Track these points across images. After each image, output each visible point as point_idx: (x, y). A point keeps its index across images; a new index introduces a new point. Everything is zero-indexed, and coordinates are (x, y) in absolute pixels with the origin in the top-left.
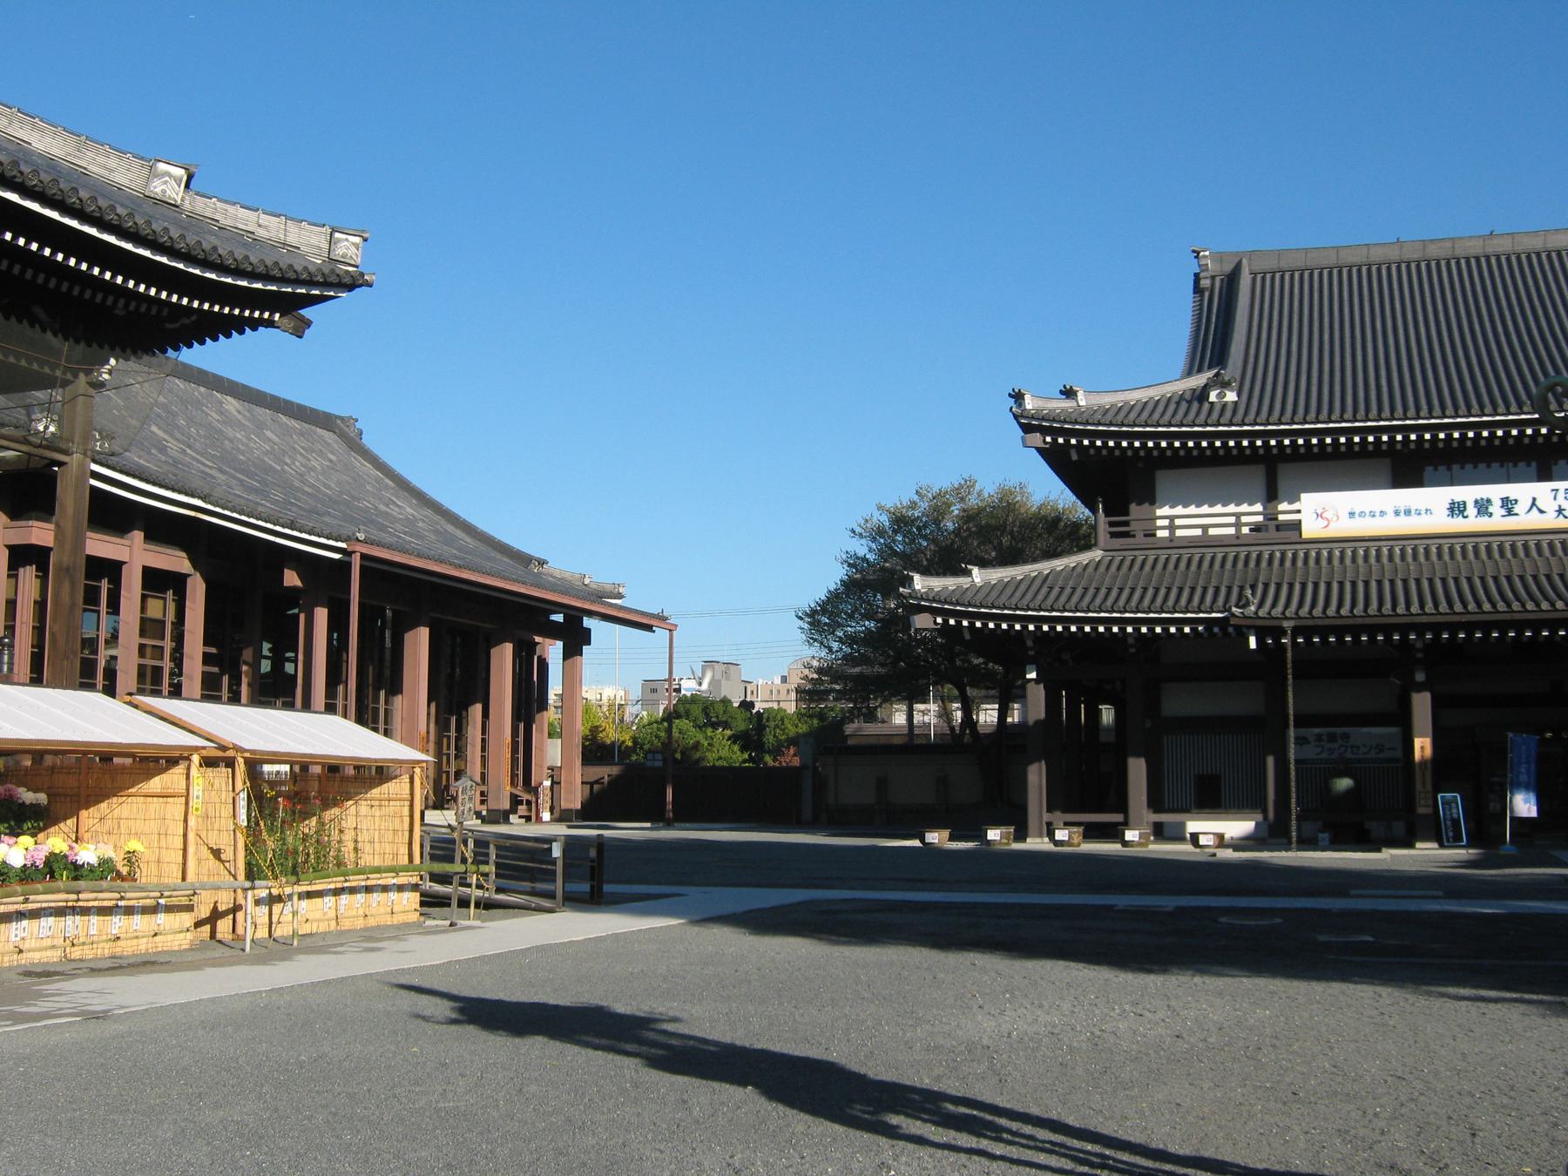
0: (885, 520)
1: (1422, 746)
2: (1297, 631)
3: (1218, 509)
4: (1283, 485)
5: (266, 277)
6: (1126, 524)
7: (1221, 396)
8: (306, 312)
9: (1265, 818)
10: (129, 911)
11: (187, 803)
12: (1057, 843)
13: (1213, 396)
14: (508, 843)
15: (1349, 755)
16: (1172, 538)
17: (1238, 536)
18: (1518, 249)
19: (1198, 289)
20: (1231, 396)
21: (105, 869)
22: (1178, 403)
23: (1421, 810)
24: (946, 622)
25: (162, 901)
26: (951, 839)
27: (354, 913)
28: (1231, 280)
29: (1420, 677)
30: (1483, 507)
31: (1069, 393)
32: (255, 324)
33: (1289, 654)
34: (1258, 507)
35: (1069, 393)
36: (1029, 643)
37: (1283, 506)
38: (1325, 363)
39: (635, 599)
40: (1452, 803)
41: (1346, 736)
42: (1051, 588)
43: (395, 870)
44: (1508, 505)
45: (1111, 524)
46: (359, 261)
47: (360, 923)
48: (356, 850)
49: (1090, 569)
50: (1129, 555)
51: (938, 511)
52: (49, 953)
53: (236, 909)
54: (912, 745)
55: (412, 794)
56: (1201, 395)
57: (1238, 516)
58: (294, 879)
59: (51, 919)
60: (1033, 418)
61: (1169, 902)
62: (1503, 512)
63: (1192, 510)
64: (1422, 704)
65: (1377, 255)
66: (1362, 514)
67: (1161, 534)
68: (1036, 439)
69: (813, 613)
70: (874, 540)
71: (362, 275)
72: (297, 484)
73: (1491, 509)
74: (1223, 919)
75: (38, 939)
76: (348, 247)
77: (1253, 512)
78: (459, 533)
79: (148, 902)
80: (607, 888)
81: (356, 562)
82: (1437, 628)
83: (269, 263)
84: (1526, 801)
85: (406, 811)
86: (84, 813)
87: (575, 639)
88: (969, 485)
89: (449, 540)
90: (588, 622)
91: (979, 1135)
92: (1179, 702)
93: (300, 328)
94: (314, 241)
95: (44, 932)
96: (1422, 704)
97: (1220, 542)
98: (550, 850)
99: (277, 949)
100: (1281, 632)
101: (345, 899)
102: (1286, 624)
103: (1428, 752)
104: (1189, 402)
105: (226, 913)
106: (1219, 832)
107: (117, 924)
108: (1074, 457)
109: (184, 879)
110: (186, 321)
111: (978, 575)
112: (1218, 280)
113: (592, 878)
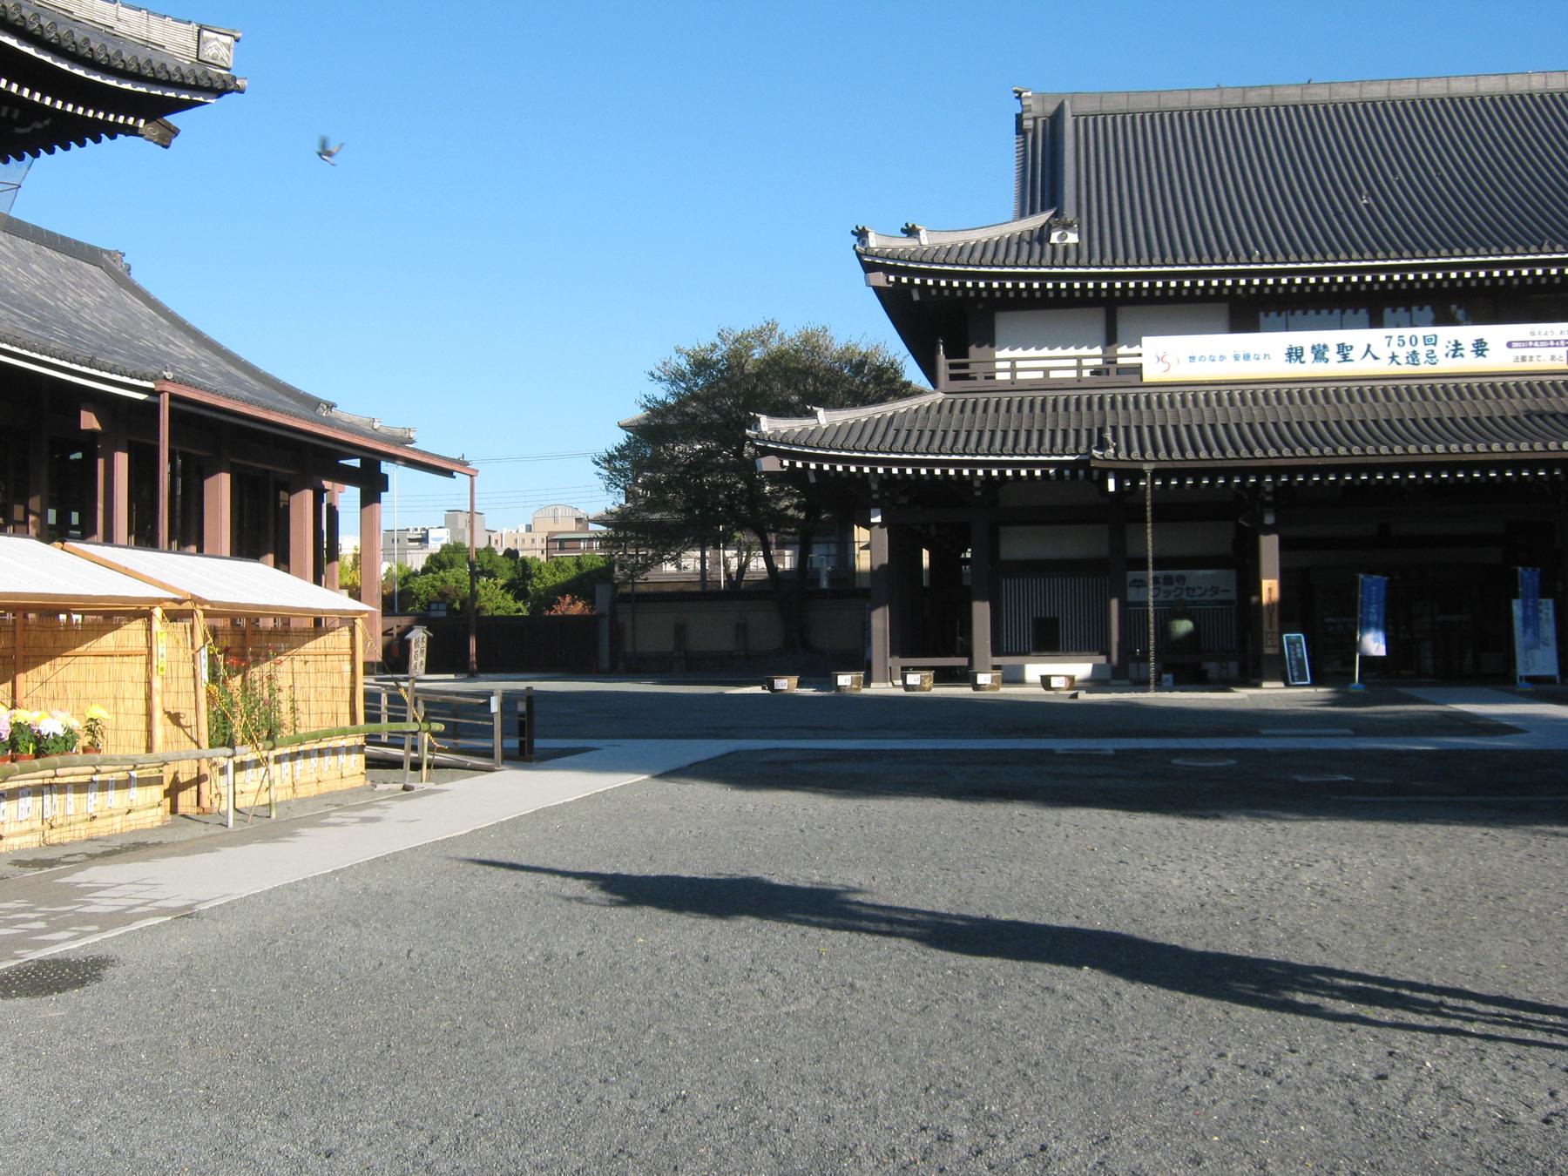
0: (684, 364)
1: (1270, 588)
2: (1156, 473)
3: (1058, 352)
4: (1122, 328)
5: (136, 77)
6: (966, 366)
7: (1063, 237)
8: (173, 119)
9: (1109, 660)
10: (104, 786)
11: (149, 663)
12: (907, 687)
14: (439, 698)
15: (1185, 596)
16: (1013, 381)
18: (1336, 98)
19: (1020, 130)
20: (1072, 238)
21: (66, 741)
22: (1019, 244)
23: (1268, 651)
24: (792, 464)
25: (134, 774)
26: (800, 685)
27: (308, 779)
28: (1055, 120)
29: (1269, 519)
30: (1319, 353)
31: (911, 232)
32: (113, 131)
33: (1149, 497)
34: (1098, 350)
35: (911, 232)
36: (874, 487)
37: (1123, 350)
38: (1162, 203)
39: (427, 442)
40: (1295, 643)
41: (1182, 579)
42: (898, 431)
43: (344, 733)
44: (1343, 350)
45: (952, 366)
46: (230, 64)
47: (314, 790)
48: (293, 710)
49: (934, 412)
50: (971, 398)
51: (736, 359)
52: (28, 838)
53: (199, 780)
54: (701, 594)
55: (353, 647)
56: (1042, 235)
57: (1079, 359)
58: (270, 744)
59: (30, 799)
60: (876, 256)
61: (1109, 745)
62: (1339, 358)
64: (1269, 546)
65: (1198, 100)
66: (1202, 358)
67: (999, 376)
68: (879, 279)
69: (610, 459)
70: (673, 383)
71: (234, 79)
72: (74, 320)
73: (1327, 355)
74: (1176, 761)
75: (18, 824)
76: (218, 48)
77: (1093, 355)
78: (244, 376)
79: (122, 776)
80: (539, 743)
81: (165, 403)
83: (142, 61)
84: (1376, 640)
85: (347, 667)
86: (21, 678)
87: (372, 486)
88: (772, 328)
89: (238, 383)
90: (386, 467)
91: (1419, 1012)
92: (1018, 545)
93: (167, 137)
94: (180, 39)
95: (24, 815)
96: (1269, 546)
97: (1061, 385)
98: (488, 705)
99: (266, 824)
100: (1141, 474)
101: (300, 763)
102: (1147, 467)
103: (1276, 595)
104: (1030, 243)
105: (188, 785)
106: (1057, 675)
107: (94, 801)
108: (916, 297)
109: (149, 749)
110: (38, 126)
111: (824, 417)
112: (1040, 122)
113: (522, 734)
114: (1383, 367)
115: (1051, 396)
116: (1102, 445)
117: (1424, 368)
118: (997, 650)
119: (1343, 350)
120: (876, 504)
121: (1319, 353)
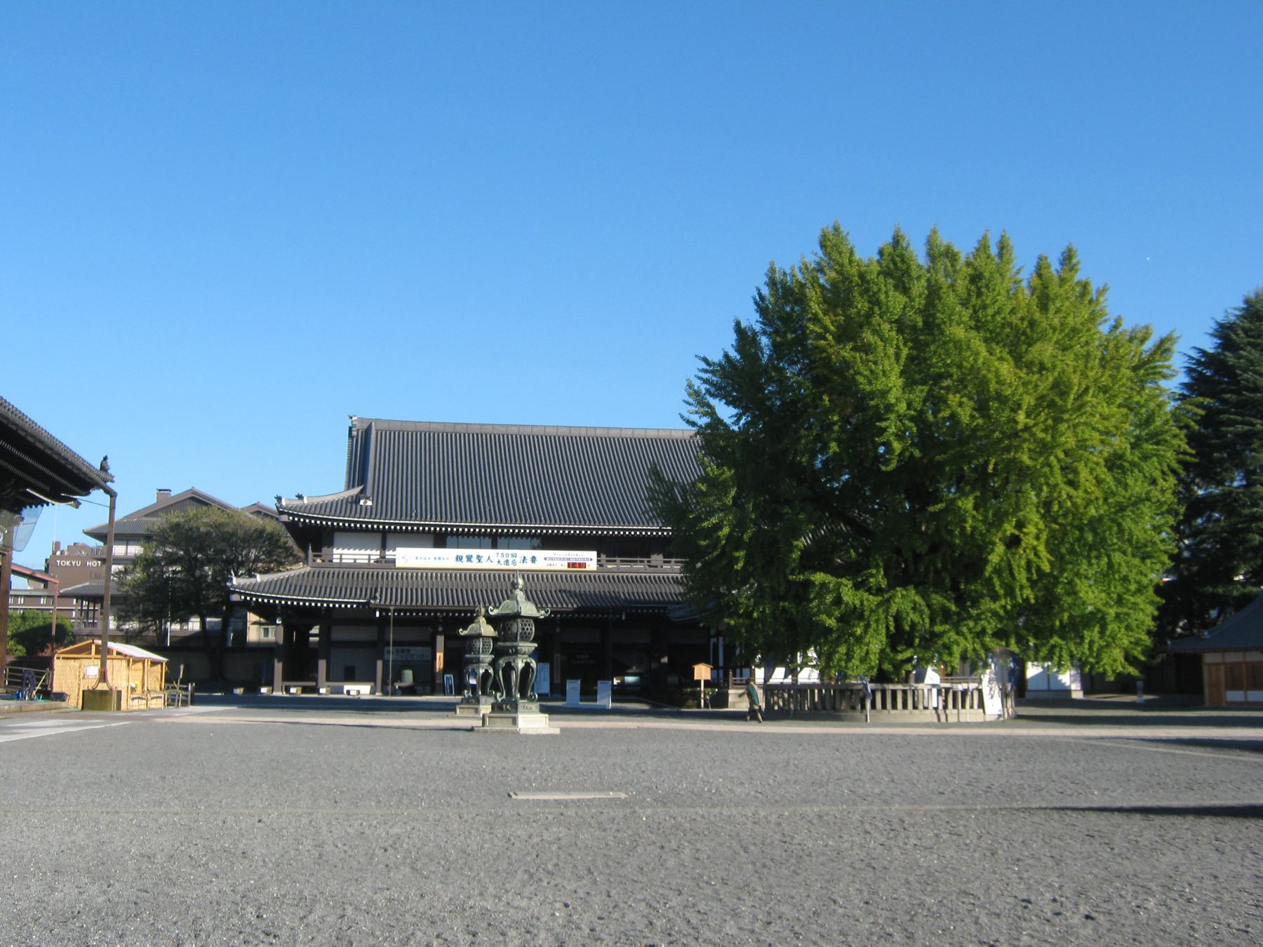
4: (389, 542)
13: (362, 502)
20: (369, 503)
28: (367, 432)
29: (440, 629)
30: (469, 558)
31: (300, 497)
40: (450, 678)
44: (479, 558)
56: (356, 500)
63: (351, 551)
64: (440, 640)
92: (338, 634)
93: (78, 505)
96: (440, 640)
97: (361, 566)
111: (259, 578)
114: (495, 566)
115: (356, 571)
116: (375, 598)
117: (511, 567)
118: (328, 679)
119: (479, 558)
120: (279, 615)
121: (469, 558)
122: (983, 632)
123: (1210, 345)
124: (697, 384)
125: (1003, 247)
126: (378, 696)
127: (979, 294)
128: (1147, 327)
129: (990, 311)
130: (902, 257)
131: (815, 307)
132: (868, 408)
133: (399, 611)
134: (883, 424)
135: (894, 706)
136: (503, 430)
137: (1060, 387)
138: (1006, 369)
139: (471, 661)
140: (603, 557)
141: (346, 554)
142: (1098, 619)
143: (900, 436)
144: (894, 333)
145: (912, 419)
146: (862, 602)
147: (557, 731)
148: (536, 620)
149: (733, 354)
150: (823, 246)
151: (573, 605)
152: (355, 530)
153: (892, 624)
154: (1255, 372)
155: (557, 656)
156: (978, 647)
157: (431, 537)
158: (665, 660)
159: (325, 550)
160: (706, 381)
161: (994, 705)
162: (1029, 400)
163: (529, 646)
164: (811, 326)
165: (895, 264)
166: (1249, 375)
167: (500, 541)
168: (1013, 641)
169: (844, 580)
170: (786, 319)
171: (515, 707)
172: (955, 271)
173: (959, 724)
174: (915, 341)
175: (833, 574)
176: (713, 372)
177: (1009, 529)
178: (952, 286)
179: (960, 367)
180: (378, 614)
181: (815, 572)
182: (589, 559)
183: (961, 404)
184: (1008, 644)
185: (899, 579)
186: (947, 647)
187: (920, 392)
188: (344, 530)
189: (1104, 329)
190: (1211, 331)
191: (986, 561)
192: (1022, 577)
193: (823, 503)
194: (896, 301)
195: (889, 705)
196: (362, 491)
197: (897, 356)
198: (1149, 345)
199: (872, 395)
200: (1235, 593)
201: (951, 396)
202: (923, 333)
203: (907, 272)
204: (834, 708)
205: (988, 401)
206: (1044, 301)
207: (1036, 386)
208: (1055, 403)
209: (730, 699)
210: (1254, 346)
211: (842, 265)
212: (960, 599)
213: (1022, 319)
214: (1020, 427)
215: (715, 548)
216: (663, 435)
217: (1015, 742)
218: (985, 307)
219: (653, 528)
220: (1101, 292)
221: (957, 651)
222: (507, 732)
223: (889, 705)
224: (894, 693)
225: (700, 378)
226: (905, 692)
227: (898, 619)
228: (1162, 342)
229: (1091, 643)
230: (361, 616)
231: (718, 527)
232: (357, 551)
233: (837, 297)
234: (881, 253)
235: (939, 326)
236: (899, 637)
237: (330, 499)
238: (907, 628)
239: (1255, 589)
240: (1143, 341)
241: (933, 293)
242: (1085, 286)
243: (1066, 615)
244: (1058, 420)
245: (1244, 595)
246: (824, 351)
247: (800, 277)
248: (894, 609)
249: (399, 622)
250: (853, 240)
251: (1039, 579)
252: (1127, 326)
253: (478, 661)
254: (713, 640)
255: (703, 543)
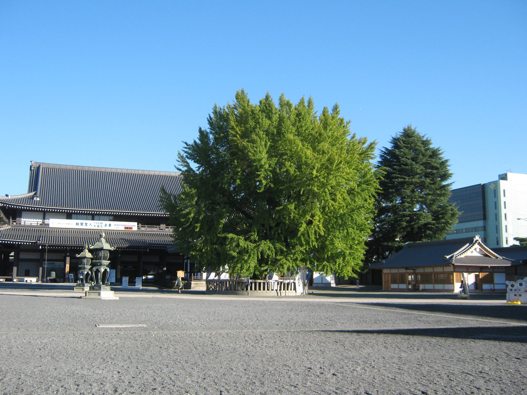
2: (48, 246)
13: (35, 199)
16: (24, 225)
17: (37, 225)
20: (38, 199)
28: (38, 168)
29: (68, 254)
30: (82, 224)
37: (47, 221)
40: (72, 276)
56: (32, 198)
63: (30, 220)
64: (68, 259)
82: (72, 247)
92: (23, 256)
96: (68, 259)
115: (32, 228)
116: (39, 240)
117: (100, 228)
119: (86, 224)
122: (297, 259)
123: (389, 146)
124: (182, 153)
125: (310, 103)
126: (40, 283)
127: (300, 121)
128: (365, 138)
129: (304, 129)
130: (269, 104)
131: (233, 123)
132: (253, 166)
133: (50, 246)
134: (259, 173)
135: (260, 289)
136: (98, 170)
137: (330, 161)
138: (309, 152)
139: (81, 268)
140: (140, 225)
141: (27, 221)
142: (342, 255)
143: (265, 178)
144: (264, 136)
145: (271, 171)
146: (248, 246)
147: (118, 298)
148: (110, 251)
149: (198, 141)
150: (237, 98)
151: (126, 245)
152: (32, 211)
153: (260, 255)
154: (407, 158)
155: (119, 266)
156: (294, 265)
157: (65, 215)
158: (165, 269)
159: (18, 219)
160: (186, 152)
161: (300, 289)
162: (318, 165)
163: (106, 262)
164: (230, 131)
165: (266, 107)
166: (404, 159)
167: (96, 217)
168: (308, 263)
169: (240, 237)
170: (221, 128)
171: (100, 288)
172: (290, 111)
173: (286, 297)
174: (273, 139)
175: (236, 234)
176: (189, 148)
177: (308, 217)
178: (289, 117)
179: (291, 151)
180: (40, 247)
181: (229, 233)
182: (134, 225)
183: (290, 166)
184: (306, 264)
185: (264, 237)
186: (282, 265)
187: (275, 160)
188: (27, 210)
189: (349, 138)
190: (390, 141)
191: (299, 230)
192: (313, 237)
193: (233, 204)
194: (266, 122)
195: (257, 289)
196: (35, 194)
197: (266, 145)
198: (366, 145)
199: (254, 161)
200: (396, 245)
201: (286, 162)
202: (276, 136)
203: (271, 111)
204: (235, 289)
205: (301, 165)
206: (325, 125)
207: (321, 160)
208: (328, 167)
209: (192, 285)
210: (407, 147)
211: (244, 107)
212: (287, 246)
213: (316, 132)
214: (314, 176)
215: (187, 223)
216: (167, 174)
217: (308, 304)
218: (302, 127)
219: (162, 213)
220: (348, 123)
221: (286, 267)
222: (96, 299)
223: (257, 289)
224: (260, 283)
225: (184, 151)
226: (264, 283)
227: (262, 253)
228: (371, 144)
229: (339, 264)
230: (33, 248)
231: (189, 213)
232: (32, 220)
233: (242, 120)
234: (261, 102)
235: (283, 134)
236: (262, 260)
237: (21, 197)
238: (266, 257)
239: (403, 244)
240: (364, 143)
241: (281, 120)
242: (342, 120)
243: (330, 253)
244: (329, 174)
245: (399, 246)
246: (236, 142)
247: (227, 110)
248: (261, 249)
249: (50, 251)
250: (249, 97)
251: (319, 238)
252: (358, 137)
253: (84, 268)
254: (185, 261)
255: (183, 220)
